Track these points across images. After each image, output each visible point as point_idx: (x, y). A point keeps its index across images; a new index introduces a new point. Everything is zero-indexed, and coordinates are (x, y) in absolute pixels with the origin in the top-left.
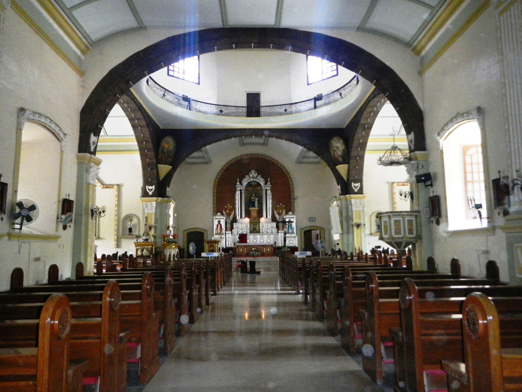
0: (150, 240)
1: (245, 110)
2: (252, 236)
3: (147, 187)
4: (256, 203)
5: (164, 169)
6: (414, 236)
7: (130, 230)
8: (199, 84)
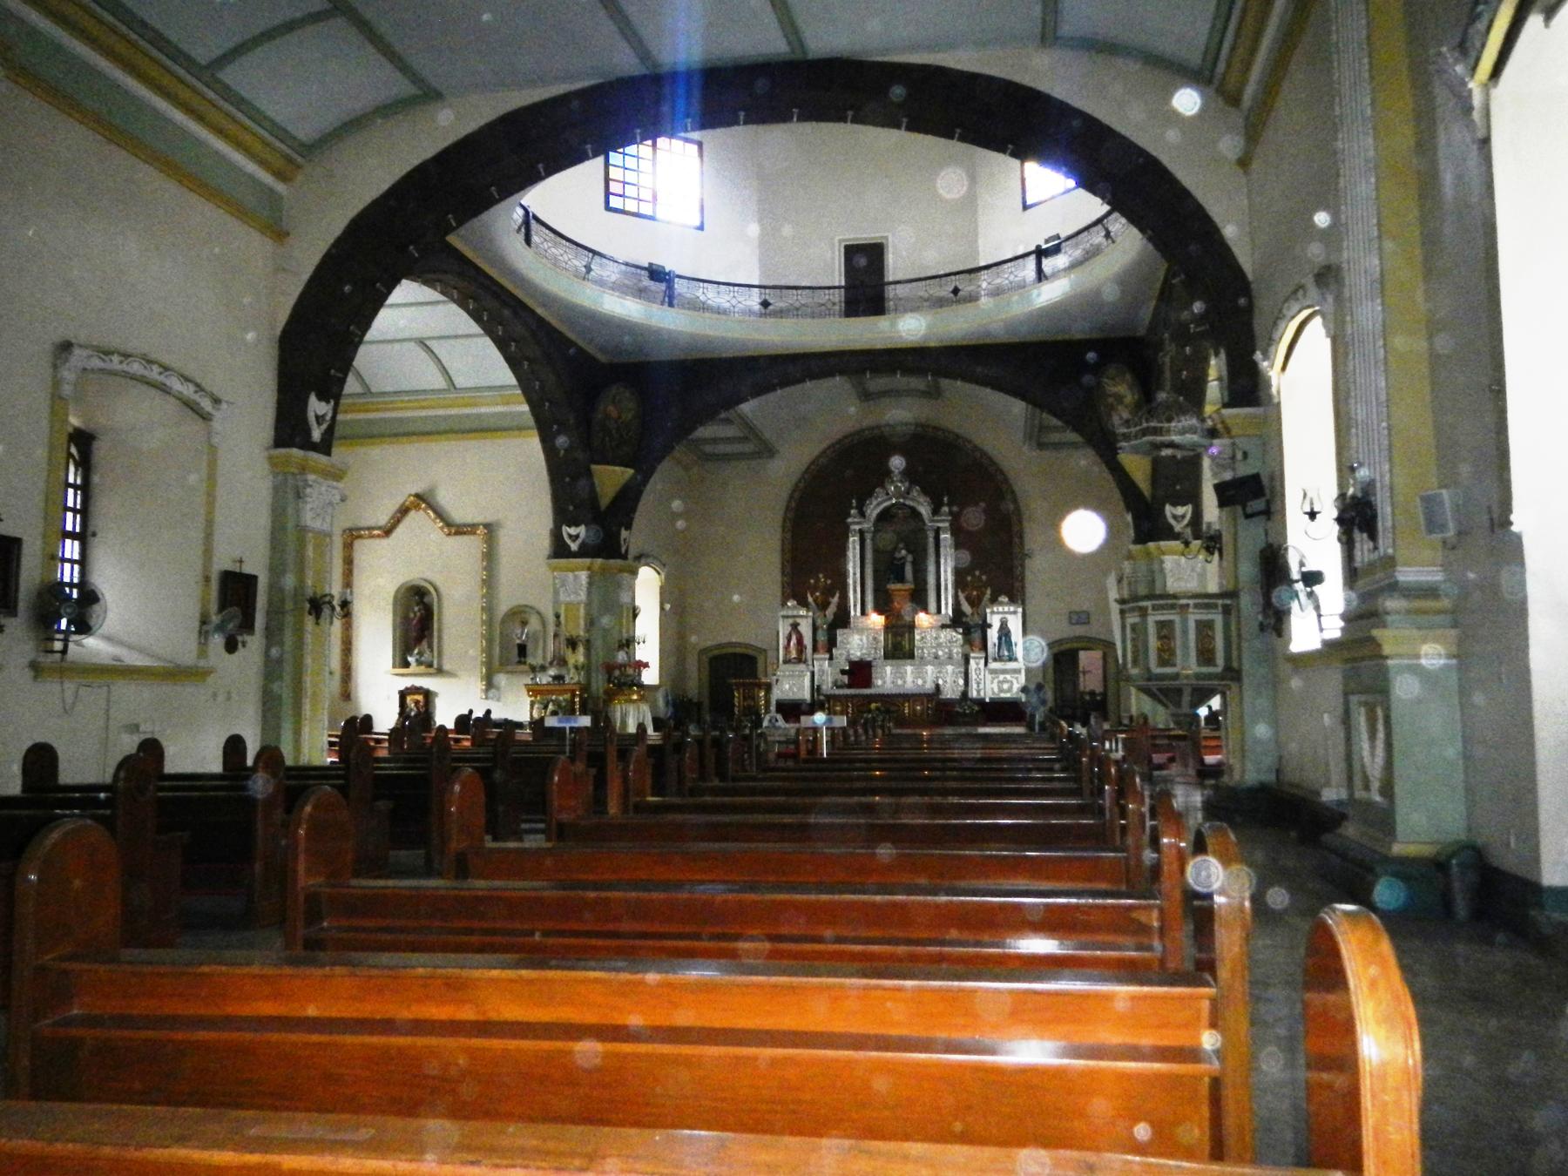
0: (567, 680)
1: (838, 297)
3: (568, 531)
4: (909, 570)
5: (610, 478)
6: (1219, 669)
7: (522, 650)
8: (701, 228)
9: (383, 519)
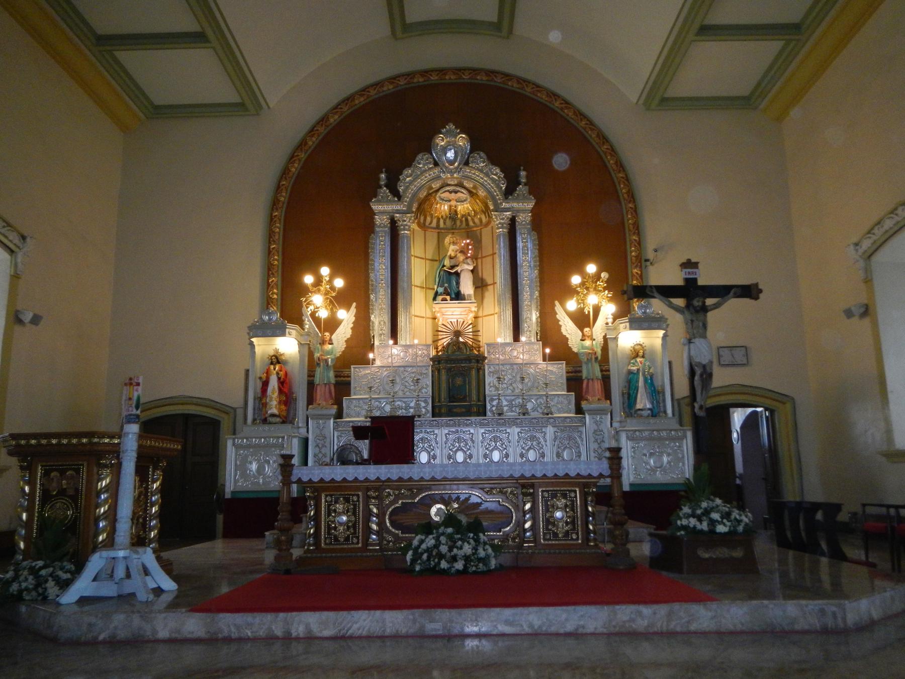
2: (441, 433)
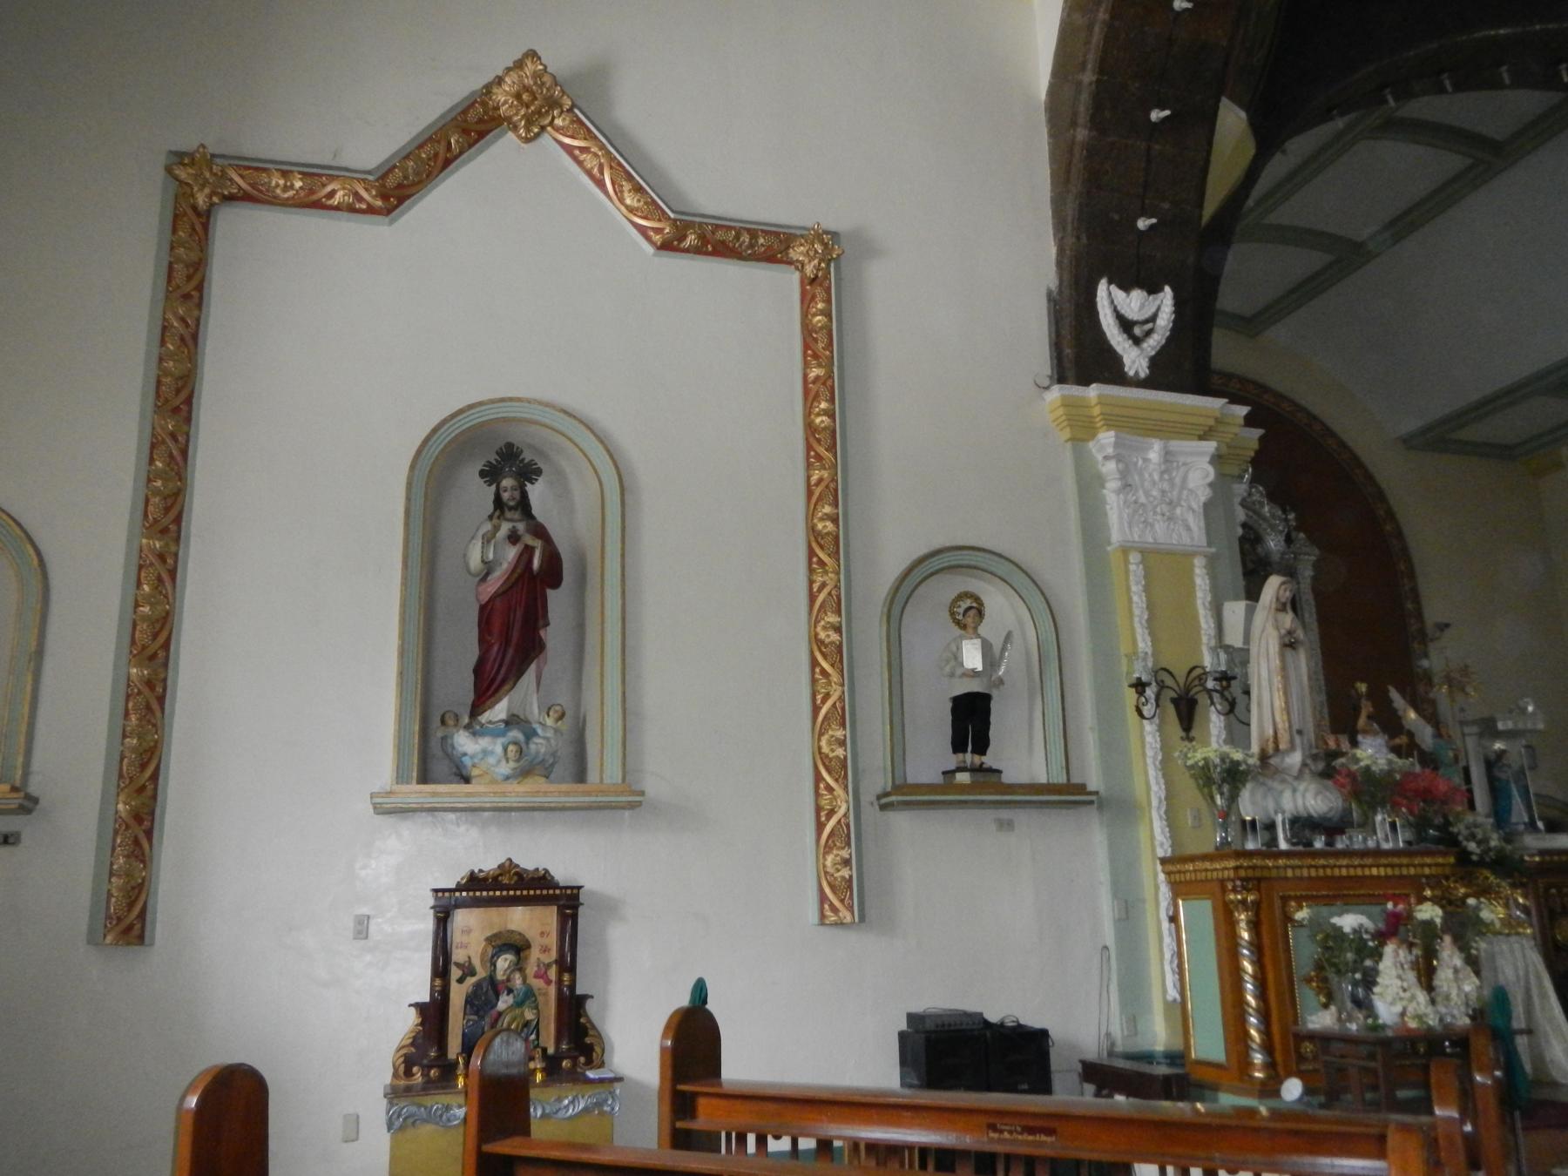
7: (971, 718)
9: (372, 145)
